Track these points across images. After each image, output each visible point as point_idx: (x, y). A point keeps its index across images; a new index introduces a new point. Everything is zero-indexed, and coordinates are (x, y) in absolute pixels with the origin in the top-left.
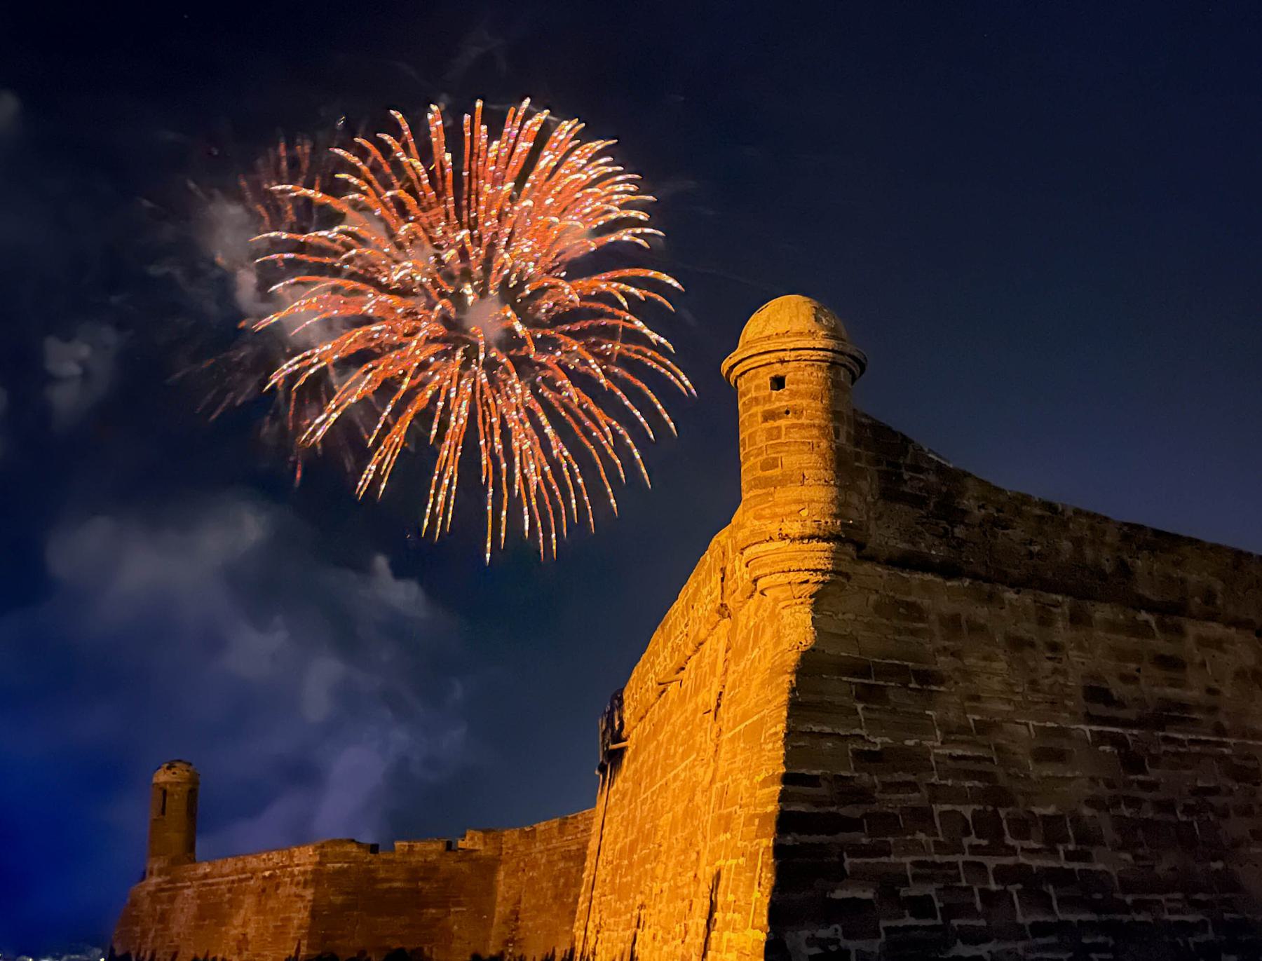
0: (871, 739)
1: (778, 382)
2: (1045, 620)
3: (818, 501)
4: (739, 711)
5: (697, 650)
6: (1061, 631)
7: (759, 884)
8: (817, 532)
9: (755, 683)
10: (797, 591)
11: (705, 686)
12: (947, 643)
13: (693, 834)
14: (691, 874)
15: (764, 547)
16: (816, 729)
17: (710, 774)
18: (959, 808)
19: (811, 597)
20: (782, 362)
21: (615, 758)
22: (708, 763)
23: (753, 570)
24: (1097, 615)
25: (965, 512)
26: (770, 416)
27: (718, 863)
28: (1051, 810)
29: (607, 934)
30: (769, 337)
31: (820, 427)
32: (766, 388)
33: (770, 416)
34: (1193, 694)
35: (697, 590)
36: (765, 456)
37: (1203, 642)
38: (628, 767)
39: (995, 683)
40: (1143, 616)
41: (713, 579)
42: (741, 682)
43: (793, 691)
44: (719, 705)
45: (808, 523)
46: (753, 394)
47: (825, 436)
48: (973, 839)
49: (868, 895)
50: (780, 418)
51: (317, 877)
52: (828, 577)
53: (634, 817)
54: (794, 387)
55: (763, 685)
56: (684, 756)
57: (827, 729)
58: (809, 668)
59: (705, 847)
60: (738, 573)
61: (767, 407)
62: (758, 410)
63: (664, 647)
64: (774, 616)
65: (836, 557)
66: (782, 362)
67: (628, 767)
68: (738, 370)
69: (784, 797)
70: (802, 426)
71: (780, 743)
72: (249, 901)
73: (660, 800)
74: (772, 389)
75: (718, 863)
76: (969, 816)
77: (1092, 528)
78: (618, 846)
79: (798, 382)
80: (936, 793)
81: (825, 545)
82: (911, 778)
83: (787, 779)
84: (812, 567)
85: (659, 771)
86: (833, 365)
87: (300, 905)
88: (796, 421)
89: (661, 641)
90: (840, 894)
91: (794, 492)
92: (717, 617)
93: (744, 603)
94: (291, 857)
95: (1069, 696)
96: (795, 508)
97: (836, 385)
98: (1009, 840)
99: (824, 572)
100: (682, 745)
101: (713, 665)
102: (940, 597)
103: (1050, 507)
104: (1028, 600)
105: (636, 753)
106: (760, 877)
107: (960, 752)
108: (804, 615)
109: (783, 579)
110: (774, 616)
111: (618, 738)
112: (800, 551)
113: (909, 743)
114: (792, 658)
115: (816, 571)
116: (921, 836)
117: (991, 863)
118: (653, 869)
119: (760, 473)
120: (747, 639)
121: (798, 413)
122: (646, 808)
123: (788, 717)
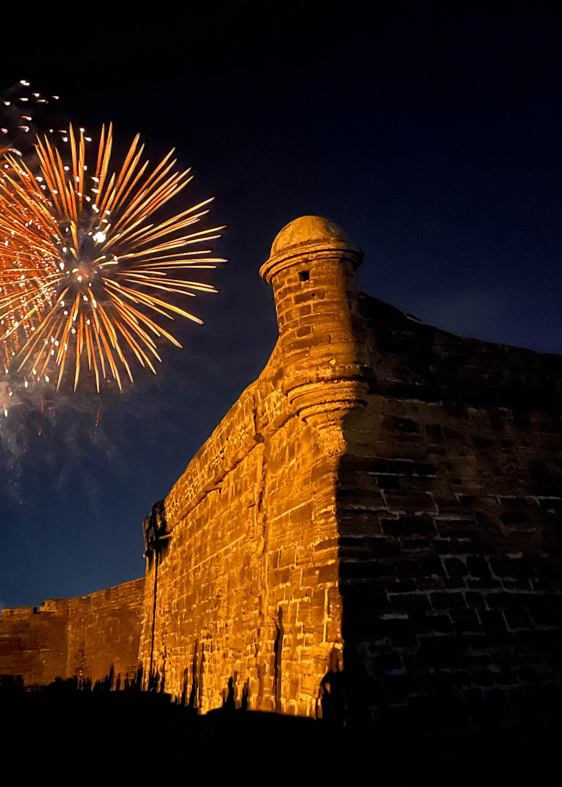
3: (342, 353)
5: (234, 467)
7: (329, 613)
9: (295, 483)
10: (330, 416)
11: (246, 489)
13: (255, 585)
14: (257, 612)
15: (305, 388)
17: (261, 548)
19: (341, 419)
21: (159, 544)
22: (259, 539)
27: (280, 603)
29: (174, 657)
32: (295, 280)
35: (232, 425)
36: (300, 327)
38: (174, 550)
41: (247, 419)
42: (281, 483)
43: (337, 483)
44: (261, 501)
45: (337, 368)
50: (309, 299)
53: (188, 582)
54: (316, 277)
55: (306, 482)
56: (232, 537)
59: (265, 594)
60: (268, 412)
61: (298, 293)
67: (174, 550)
69: (341, 554)
70: (325, 304)
71: (333, 518)
73: (213, 569)
74: (301, 280)
75: (280, 603)
79: (319, 274)
83: (341, 542)
84: (341, 398)
85: (208, 549)
89: (198, 465)
91: (323, 350)
93: (275, 431)
96: (325, 359)
99: (349, 401)
100: (229, 530)
101: (255, 474)
105: (181, 541)
106: (328, 608)
108: (337, 433)
109: (320, 408)
112: (332, 388)
114: (332, 461)
115: (343, 401)
118: (215, 613)
119: (298, 338)
121: (321, 294)
122: (199, 574)
123: (337, 500)
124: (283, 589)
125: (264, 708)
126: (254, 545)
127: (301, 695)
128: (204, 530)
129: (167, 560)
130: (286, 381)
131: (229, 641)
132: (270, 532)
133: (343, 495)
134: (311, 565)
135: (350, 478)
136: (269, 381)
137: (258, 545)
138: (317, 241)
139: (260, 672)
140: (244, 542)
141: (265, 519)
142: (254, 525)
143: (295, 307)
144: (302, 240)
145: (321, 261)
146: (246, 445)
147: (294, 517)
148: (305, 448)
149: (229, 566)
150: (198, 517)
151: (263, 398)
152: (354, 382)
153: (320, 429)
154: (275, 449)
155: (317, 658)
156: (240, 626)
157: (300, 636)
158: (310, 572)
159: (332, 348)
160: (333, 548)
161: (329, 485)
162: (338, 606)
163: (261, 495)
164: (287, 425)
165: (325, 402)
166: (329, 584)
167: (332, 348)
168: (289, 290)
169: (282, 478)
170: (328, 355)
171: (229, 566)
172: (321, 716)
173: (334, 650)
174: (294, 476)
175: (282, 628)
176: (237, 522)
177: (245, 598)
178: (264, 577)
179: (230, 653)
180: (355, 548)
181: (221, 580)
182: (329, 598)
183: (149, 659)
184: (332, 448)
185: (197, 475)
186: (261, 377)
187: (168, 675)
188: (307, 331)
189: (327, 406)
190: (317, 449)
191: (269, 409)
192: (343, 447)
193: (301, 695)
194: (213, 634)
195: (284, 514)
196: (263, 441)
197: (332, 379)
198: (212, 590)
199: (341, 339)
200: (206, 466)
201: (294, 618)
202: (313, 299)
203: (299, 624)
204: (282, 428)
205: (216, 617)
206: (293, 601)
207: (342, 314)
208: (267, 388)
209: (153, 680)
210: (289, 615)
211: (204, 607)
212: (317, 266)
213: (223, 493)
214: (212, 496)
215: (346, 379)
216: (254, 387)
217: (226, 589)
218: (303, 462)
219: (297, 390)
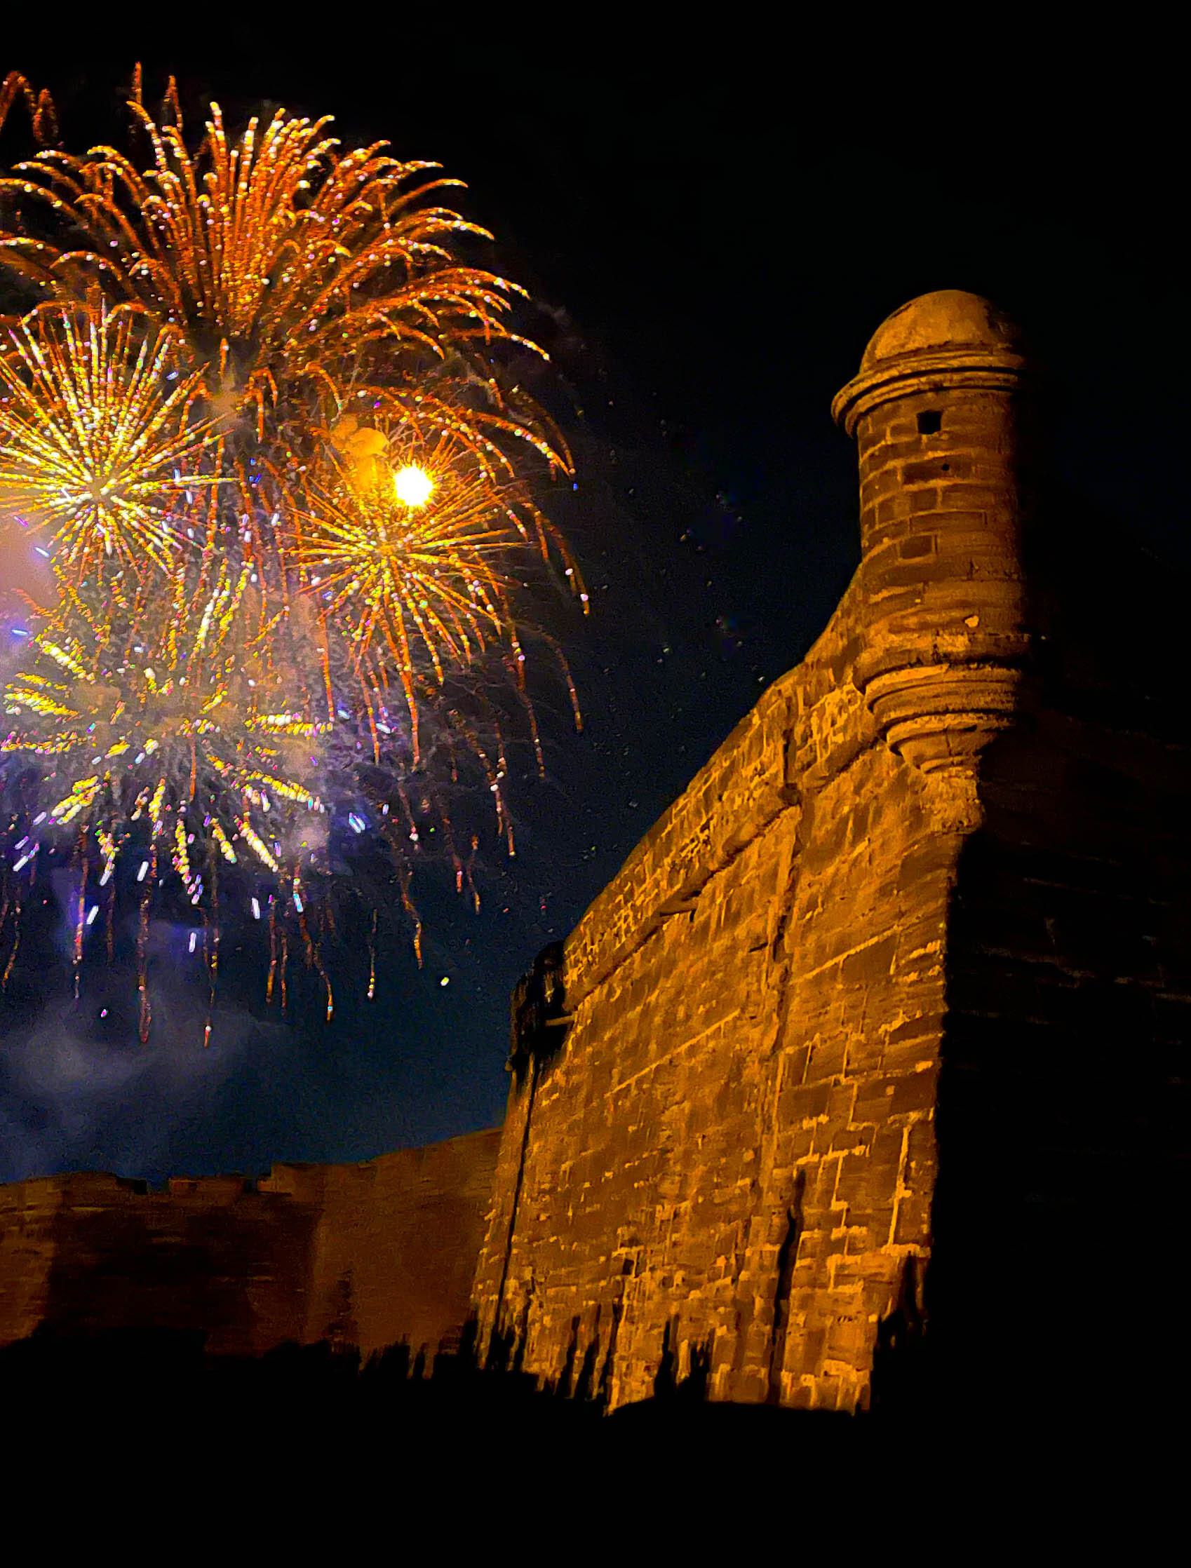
1: (929, 422)
4: (831, 937)
5: (729, 860)
7: (905, 1180)
8: (993, 649)
9: (861, 894)
10: (954, 743)
11: (750, 911)
14: (748, 1181)
19: (976, 753)
21: (542, 1039)
22: (769, 1018)
23: (882, 713)
26: (913, 474)
27: (802, 1161)
41: (767, 751)
42: (828, 894)
44: (780, 937)
46: (889, 440)
51: (58, 1226)
52: (1005, 723)
53: (602, 1121)
54: (956, 428)
55: (884, 892)
56: (708, 1019)
57: (1006, 953)
59: (770, 1142)
60: (816, 737)
61: (913, 460)
63: (657, 864)
64: (901, 784)
65: (1019, 690)
67: (575, 1053)
69: (946, 1048)
70: (968, 489)
75: (802, 1161)
78: (565, 1166)
79: (964, 421)
81: (1001, 672)
84: (982, 704)
85: (653, 1047)
87: (33, 1264)
88: (959, 481)
89: (648, 858)
91: (957, 591)
92: (780, 804)
93: (828, 780)
94: (21, 1197)
96: (956, 614)
99: (999, 714)
101: (775, 874)
105: (593, 1032)
106: (908, 1167)
109: (934, 724)
114: (951, 844)
115: (987, 711)
119: (901, 561)
120: (839, 832)
124: (809, 1131)
125: (740, 1397)
126: (755, 1034)
127: (828, 1365)
128: (647, 1006)
129: (558, 1075)
130: (865, 658)
131: (678, 1250)
132: (795, 1005)
134: (878, 1075)
136: (826, 665)
137: (764, 1034)
138: (967, 346)
139: (740, 1319)
140: (734, 1027)
141: (786, 975)
142: (759, 990)
144: (932, 342)
145: (971, 393)
146: (760, 809)
147: (852, 970)
148: (891, 816)
150: (636, 976)
151: (808, 703)
152: (1013, 671)
153: (928, 772)
154: (823, 821)
155: (871, 1282)
156: (705, 1215)
157: (837, 1233)
158: (874, 1090)
159: (972, 591)
160: (931, 1036)
161: (936, 898)
162: (930, 1163)
163: (783, 922)
164: (856, 766)
165: (946, 712)
166: (914, 1116)
168: (892, 452)
169: (833, 885)
170: (963, 605)
172: (866, 1405)
173: (911, 1261)
174: (860, 880)
175: (802, 1218)
176: (724, 985)
177: (724, 1152)
178: (771, 1104)
179: (678, 1277)
182: (910, 1146)
183: (495, 1297)
184: (951, 814)
185: (648, 879)
186: (810, 658)
187: (534, 1332)
188: (922, 547)
189: (950, 721)
190: (917, 816)
191: (820, 730)
192: (976, 817)
193: (828, 1365)
194: (644, 1236)
195: (830, 964)
196: (799, 803)
197: (967, 660)
198: (654, 1135)
199: (996, 571)
200: (667, 861)
201: (828, 1193)
202: (945, 476)
203: (837, 1206)
204: (843, 775)
205: (657, 1198)
206: (831, 1155)
207: (1004, 517)
208: (819, 683)
210: (819, 1186)
211: (632, 1175)
213: (699, 919)
214: (673, 927)
216: (791, 681)
217: (683, 1134)
218: (885, 845)
219: (886, 679)
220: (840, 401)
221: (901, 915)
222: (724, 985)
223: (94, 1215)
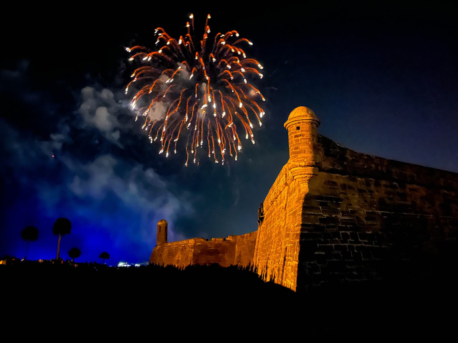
0: (324, 215)
1: (298, 128)
2: (368, 184)
6: (372, 187)
12: (343, 191)
13: (280, 238)
16: (310, 213)
18: (347, 232)
20: (299, 123)
21: (262, 219)
24: (382, 183)
25: (347, 158)
26: (296, 136)
28: (370, 232)
30: (295, 117)
31: (309, 139)
33: (296, 136)
34: (409, 203)
35: (280, 179)
37: (411, 189)
39: (356, 201)
40: (395, 183)
43: (303, 204)
46: (292, 131)
47: (310, 141)
48: (350, 240)
49: (324, 253)
51: (194, 246)
55: (296, 202)
56: (278, 219)
58: (308, 198)
61: (295, 134)
62: (293, 135)
65: (313, 171)
66: (299, 123)
68: (288, 126)
69: (302, 230)
70: (304, 139)
72: (179, 252)
76: (349, 234)
77: (380, 161)
79: (303, 128)
80: (341, 228)
81: (311, 168)
82: (333, 225)
83: (302, 225)
86: (312, 123)
87: (191, 253)
90: (316, 253)
92: (285, 186)
94: (188, 242)
95: (375, 204)
96: (303, 159)
97: (313, 128)
98: (360, 240)
99: (311, 174)
101: (284, 197)
102: (340, 179)
103: (368, 156)
104: (364, 180)
107: (346, 218)
109: (300, 176)
110: (299, 185)
111: (262, 214)
113: (334, 216)
114: (303, 196)
116: (337, 239)
117: (355, 245)
119: (294, 151)
121: (303, 135)
123: (303, 210)
125: (279, 283)
127: (287, 280)
133: (306, 207)
135: (309, 202)
139: (279, 270)
143: (294, 139)
147: (292, 214)
148: (297, 189)
149: (276, 229)
155: (292, 266)
156: (276, 252)
157: (289, 258)
159: (305, 155)
166: (297, 240)
167: (305, 155)
170: (304, 157)
171: (276, 229)
180: (308, 228)
181: (274, 234)
185: (271, 195)
190: (300, 190)
192: (308, 190)
207: (310, 143)
209: (256, 269)
212: (303, 125)
214: (275, 203)
215: (309, 166)
218: (296, 195)
220: (285, 125)
221: (298, 206)
222: (279, 214)
223: (199, 245)
